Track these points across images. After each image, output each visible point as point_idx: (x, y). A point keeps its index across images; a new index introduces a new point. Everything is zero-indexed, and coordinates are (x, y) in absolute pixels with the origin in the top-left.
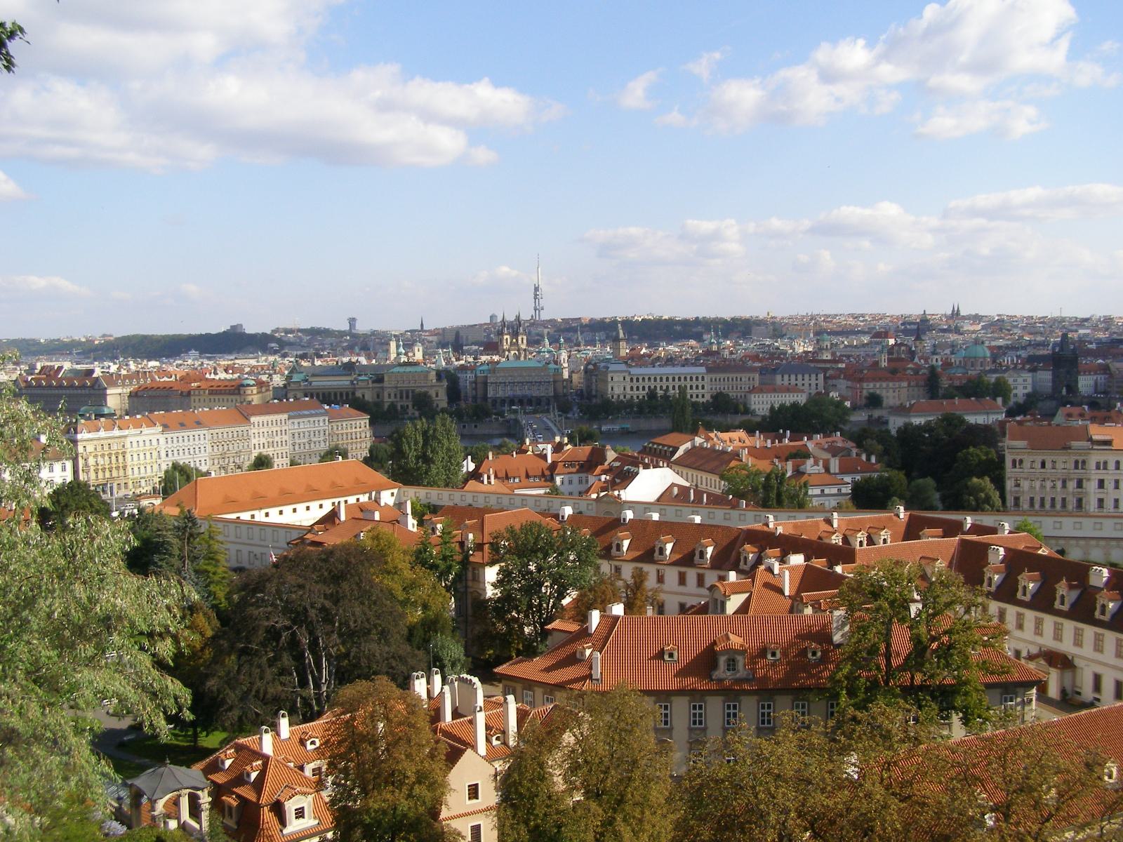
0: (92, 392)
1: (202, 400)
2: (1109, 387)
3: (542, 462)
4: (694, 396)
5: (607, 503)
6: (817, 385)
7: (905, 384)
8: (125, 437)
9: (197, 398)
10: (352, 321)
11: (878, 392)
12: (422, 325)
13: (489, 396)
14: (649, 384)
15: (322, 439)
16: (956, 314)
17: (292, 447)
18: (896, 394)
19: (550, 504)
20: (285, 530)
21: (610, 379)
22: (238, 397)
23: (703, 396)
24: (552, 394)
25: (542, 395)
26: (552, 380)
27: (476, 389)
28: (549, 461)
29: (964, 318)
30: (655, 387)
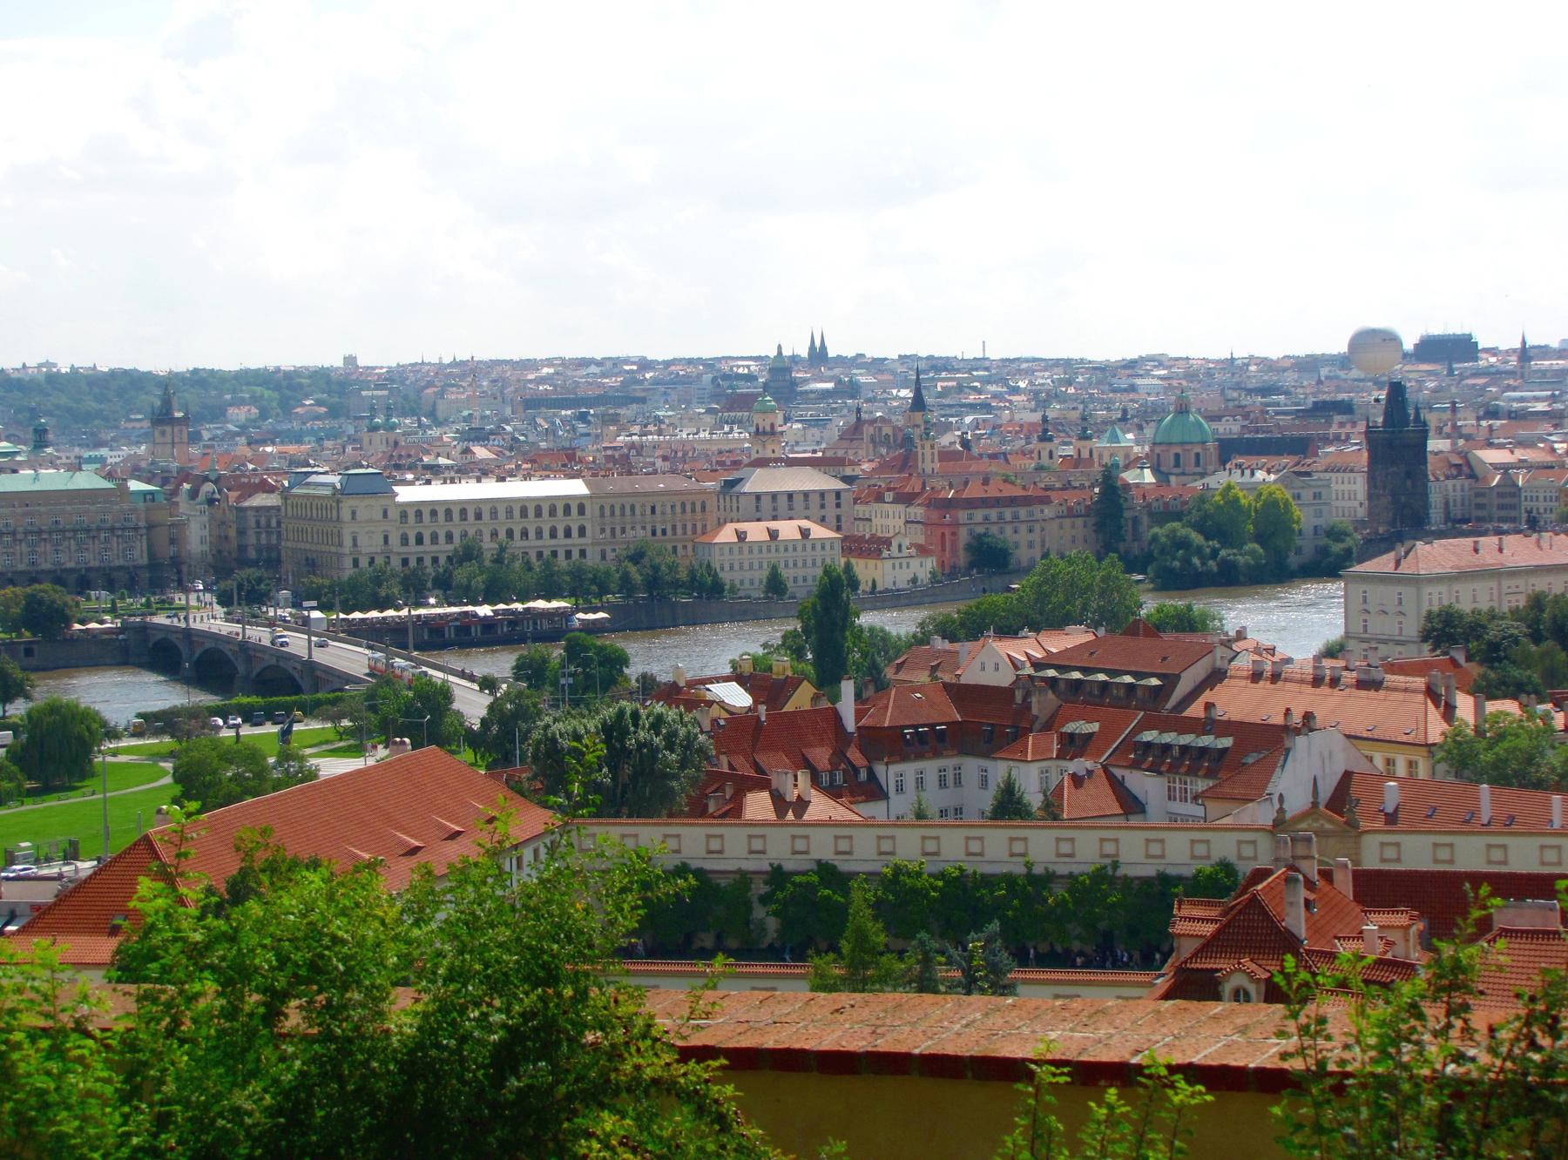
2: (1480, 506)
6: (838, 518)
7: (1048, 512)
11: (994, 530)
16: (818, 355)
19: (1109, 848)
21: (346, 514)
23: (583, 553)
24: (145, 561)
25: (121, 562)
26: (142, 524)
30: (479, 532)
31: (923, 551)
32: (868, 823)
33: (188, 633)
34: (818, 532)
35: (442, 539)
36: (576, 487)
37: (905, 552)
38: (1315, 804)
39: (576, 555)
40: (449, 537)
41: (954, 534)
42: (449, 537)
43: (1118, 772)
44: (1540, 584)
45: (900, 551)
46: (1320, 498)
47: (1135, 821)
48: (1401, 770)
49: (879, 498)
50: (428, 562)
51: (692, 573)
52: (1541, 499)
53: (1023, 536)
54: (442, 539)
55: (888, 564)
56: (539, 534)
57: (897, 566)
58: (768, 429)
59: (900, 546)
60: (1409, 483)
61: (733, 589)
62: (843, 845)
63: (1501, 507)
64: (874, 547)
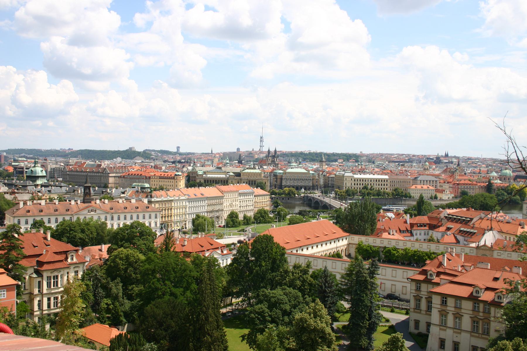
0: (102, 175)
1: (156, 181)
3: (405, 225)
4: (385, 189)
5: (482, 249)
8: (172, 201)
9: (153, 180)
10: (178, 148)
11: (466, 190)
12: (212, 151)
13: (283, 184)
14: (360, 182)
15: (251, 204)
16: (447, 155)
17: (239, 208)
18: (474, 191)
20: (296, 256)
21: (345, 179)
22: (173, 180)
23: (387, 189)
24: (312, 185)
27: (276, 181)
28: (408, 222)
29: (452, 157)
30: (368, 184)
31: (451, 193)
32: (410, 241)
33: (313, 198)
34: (431, 188)
35: (361, 185)
36: (386, 177)
37: (447, 193)
38: (485, 244)
39: (383, 189)
40: (363, 184)
42: (363, 184)
43: (456, 235)
47: (458, 244)
48: (508, 239)
49: (445, 182)
50: (359, 188)
51: (406, 194)
53: (471, 191)
54: (361, 185)
55: (444, 195)
56: (382, 185)
61: (413, 197)
62: (397, 243)
64: (442, 191)
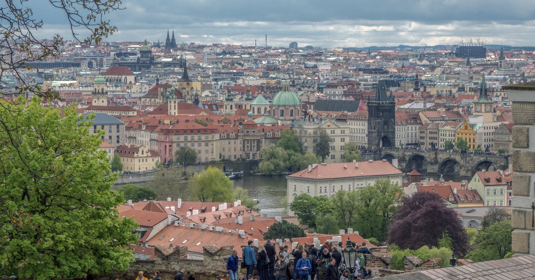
2: (422, 138)
7: (217, 136)
18: (209, 148)
31: (154, 154)
41: (170, 146)
44: (346, 186)
45: (143, 153)
46: (344, 133)
52: (448, 135)
55: (137, 160)
57: (141, 160)
58: (100, 91)
59: (143, 151)
60: (386, 127)
63: (431, 138)
